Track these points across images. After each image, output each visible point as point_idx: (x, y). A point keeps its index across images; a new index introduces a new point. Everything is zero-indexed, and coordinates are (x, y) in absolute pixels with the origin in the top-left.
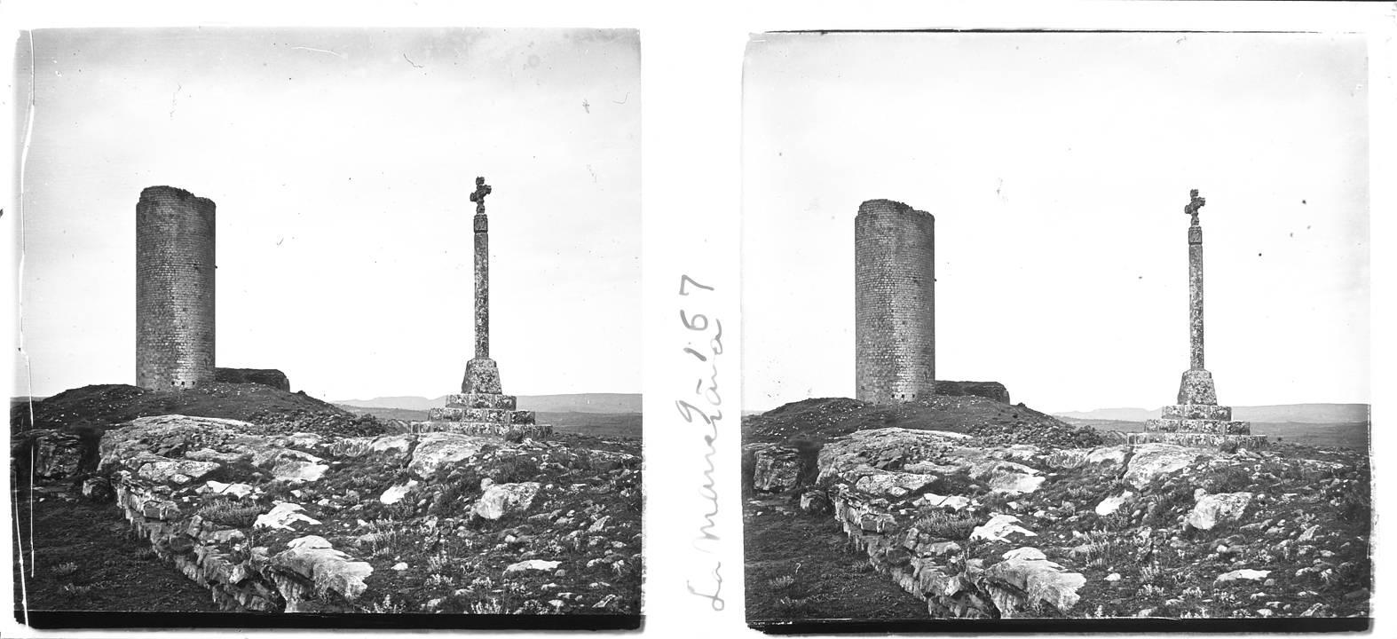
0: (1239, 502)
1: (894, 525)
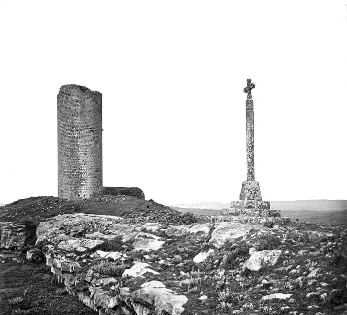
0: (274, 255)
1: (79, 268)
